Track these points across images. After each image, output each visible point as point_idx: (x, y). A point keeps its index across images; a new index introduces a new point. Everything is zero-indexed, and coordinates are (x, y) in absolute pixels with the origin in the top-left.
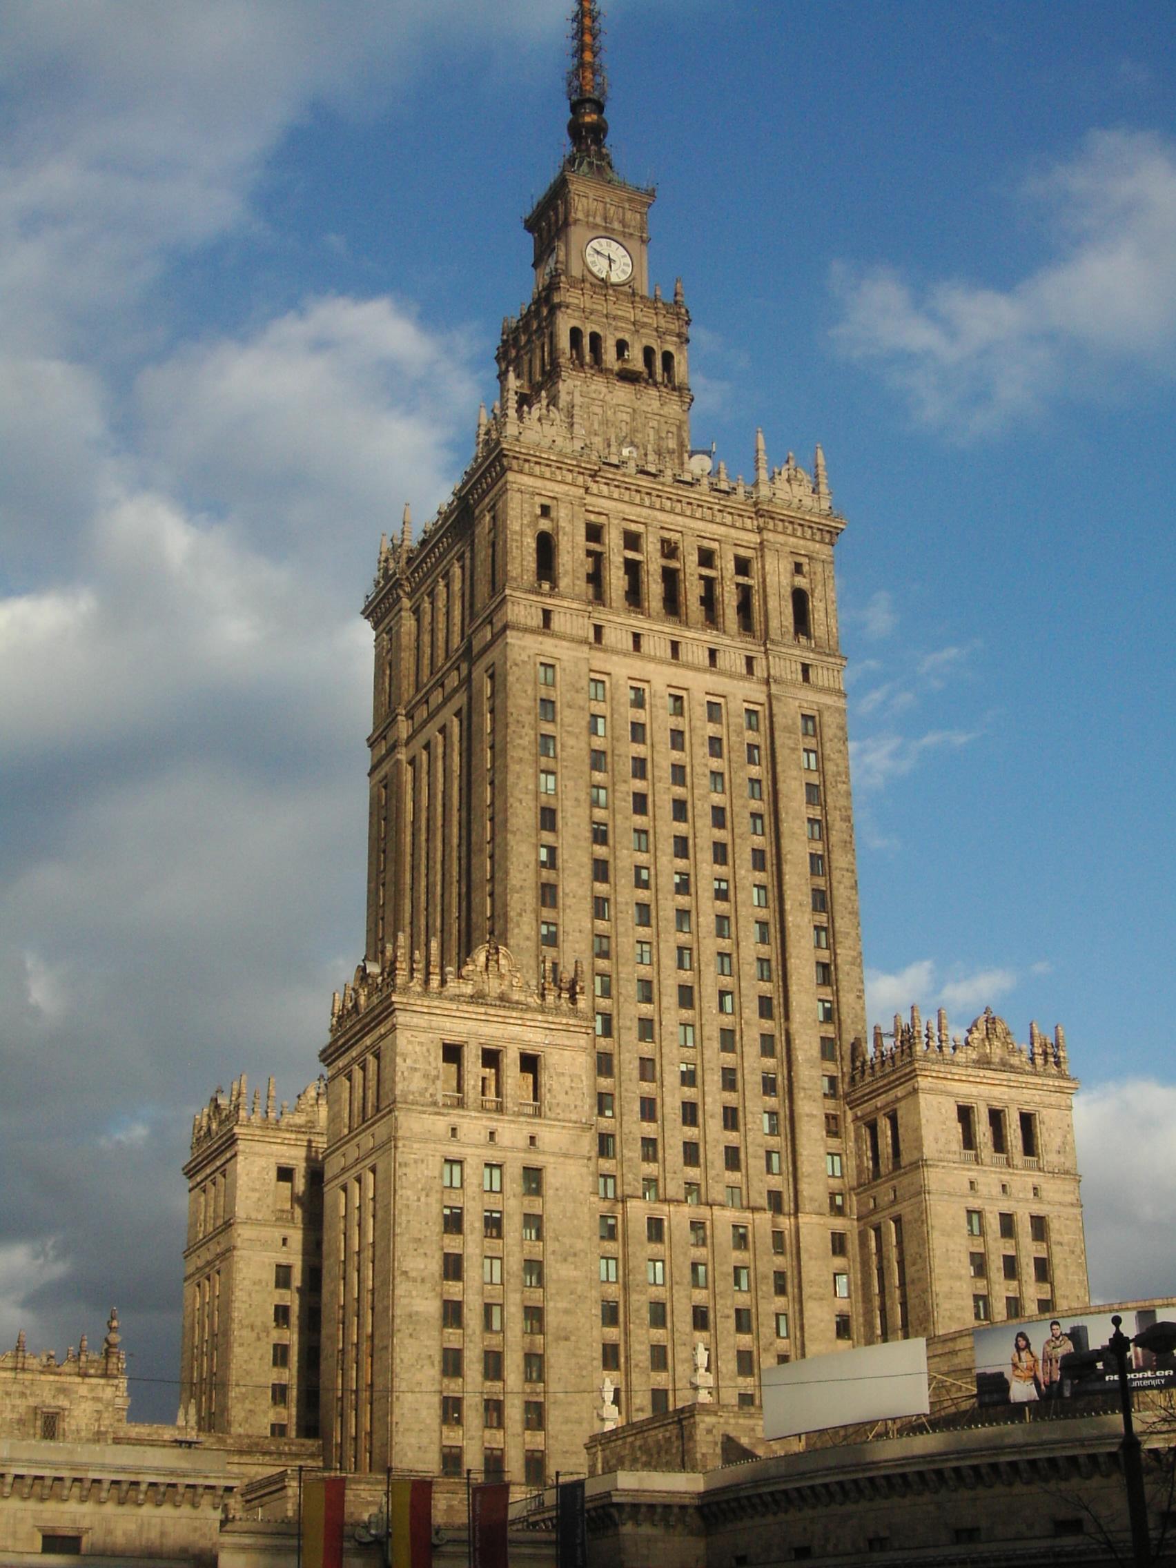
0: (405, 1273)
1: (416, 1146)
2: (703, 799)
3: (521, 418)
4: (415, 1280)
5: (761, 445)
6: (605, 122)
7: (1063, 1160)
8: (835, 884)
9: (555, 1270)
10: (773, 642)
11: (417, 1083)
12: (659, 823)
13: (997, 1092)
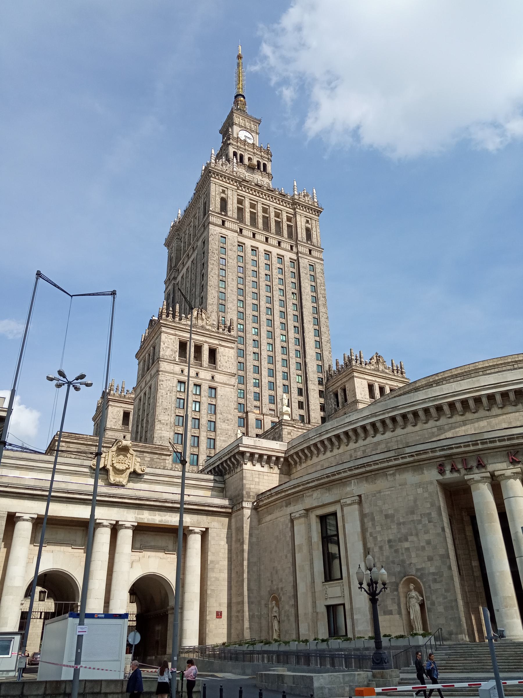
0: (160, 421)
5: (295, 184)
8: (321, 317)
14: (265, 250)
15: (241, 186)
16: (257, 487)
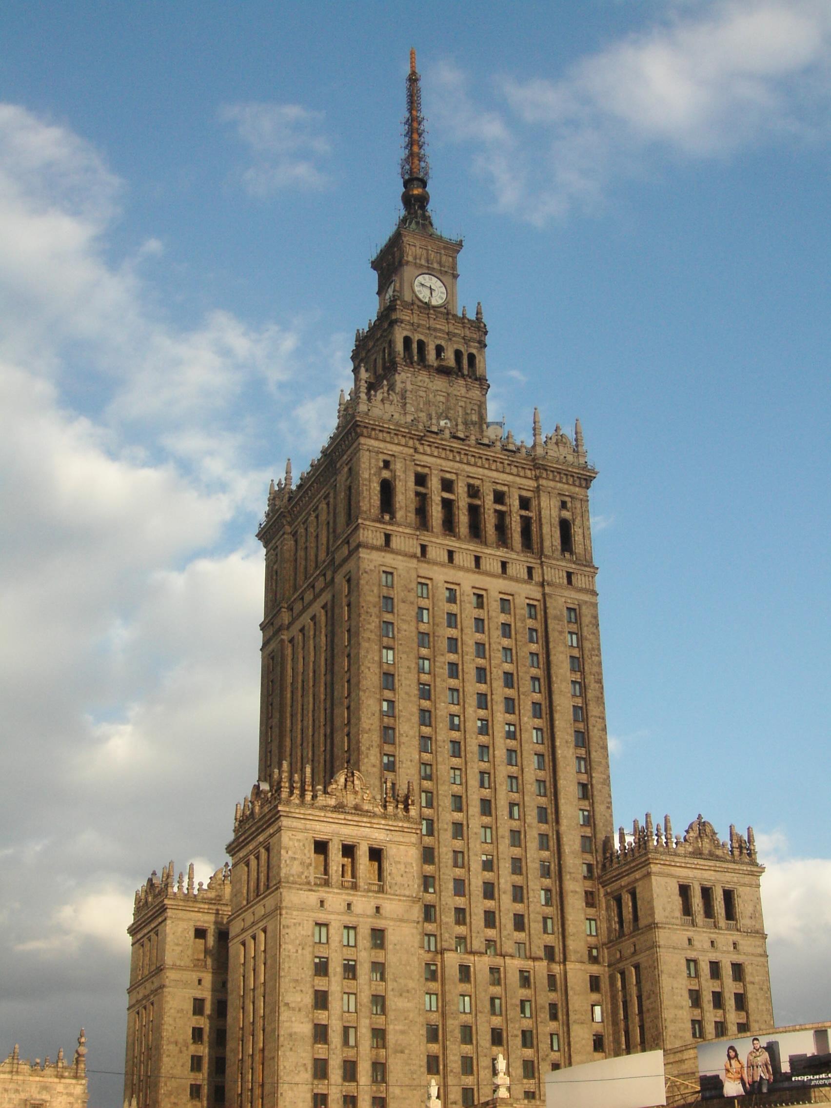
0: (287, 1004)
1: (295, 913)
2: (499, 666)
3: (369, 399)
4: (294, 1009)
6: (427, 193)
7: (754, 923)
8: (591, 727)
9: (394, 1002)
10: (546, 556)
11: (296, 868)
12: (467, 684)
13: (707, 875)
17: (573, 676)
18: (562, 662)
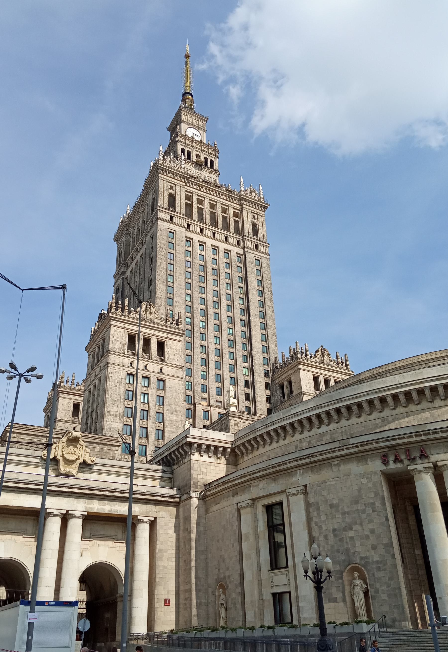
0: (109, 412)
4: (113, 415)
5: (242, 180)
8: (267, 310)
14: (212, 245)
15: (189, 183)
16: (204, 477)
17: (258, 287)
18: (253, 281)
